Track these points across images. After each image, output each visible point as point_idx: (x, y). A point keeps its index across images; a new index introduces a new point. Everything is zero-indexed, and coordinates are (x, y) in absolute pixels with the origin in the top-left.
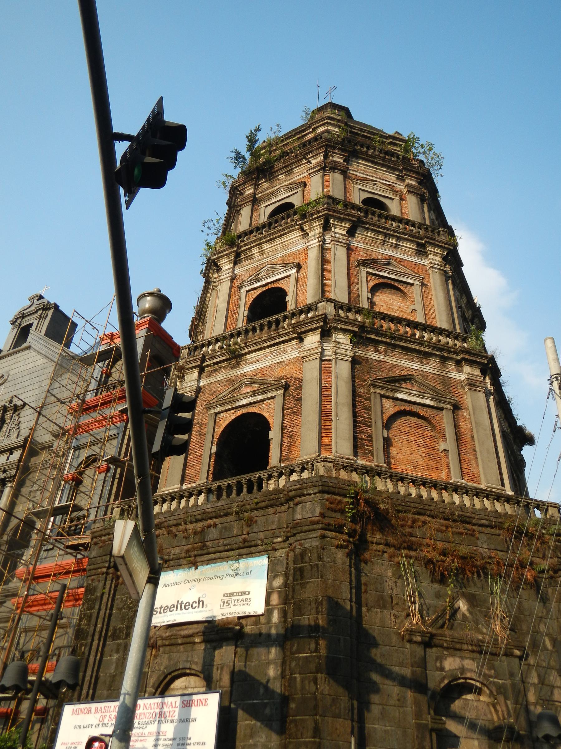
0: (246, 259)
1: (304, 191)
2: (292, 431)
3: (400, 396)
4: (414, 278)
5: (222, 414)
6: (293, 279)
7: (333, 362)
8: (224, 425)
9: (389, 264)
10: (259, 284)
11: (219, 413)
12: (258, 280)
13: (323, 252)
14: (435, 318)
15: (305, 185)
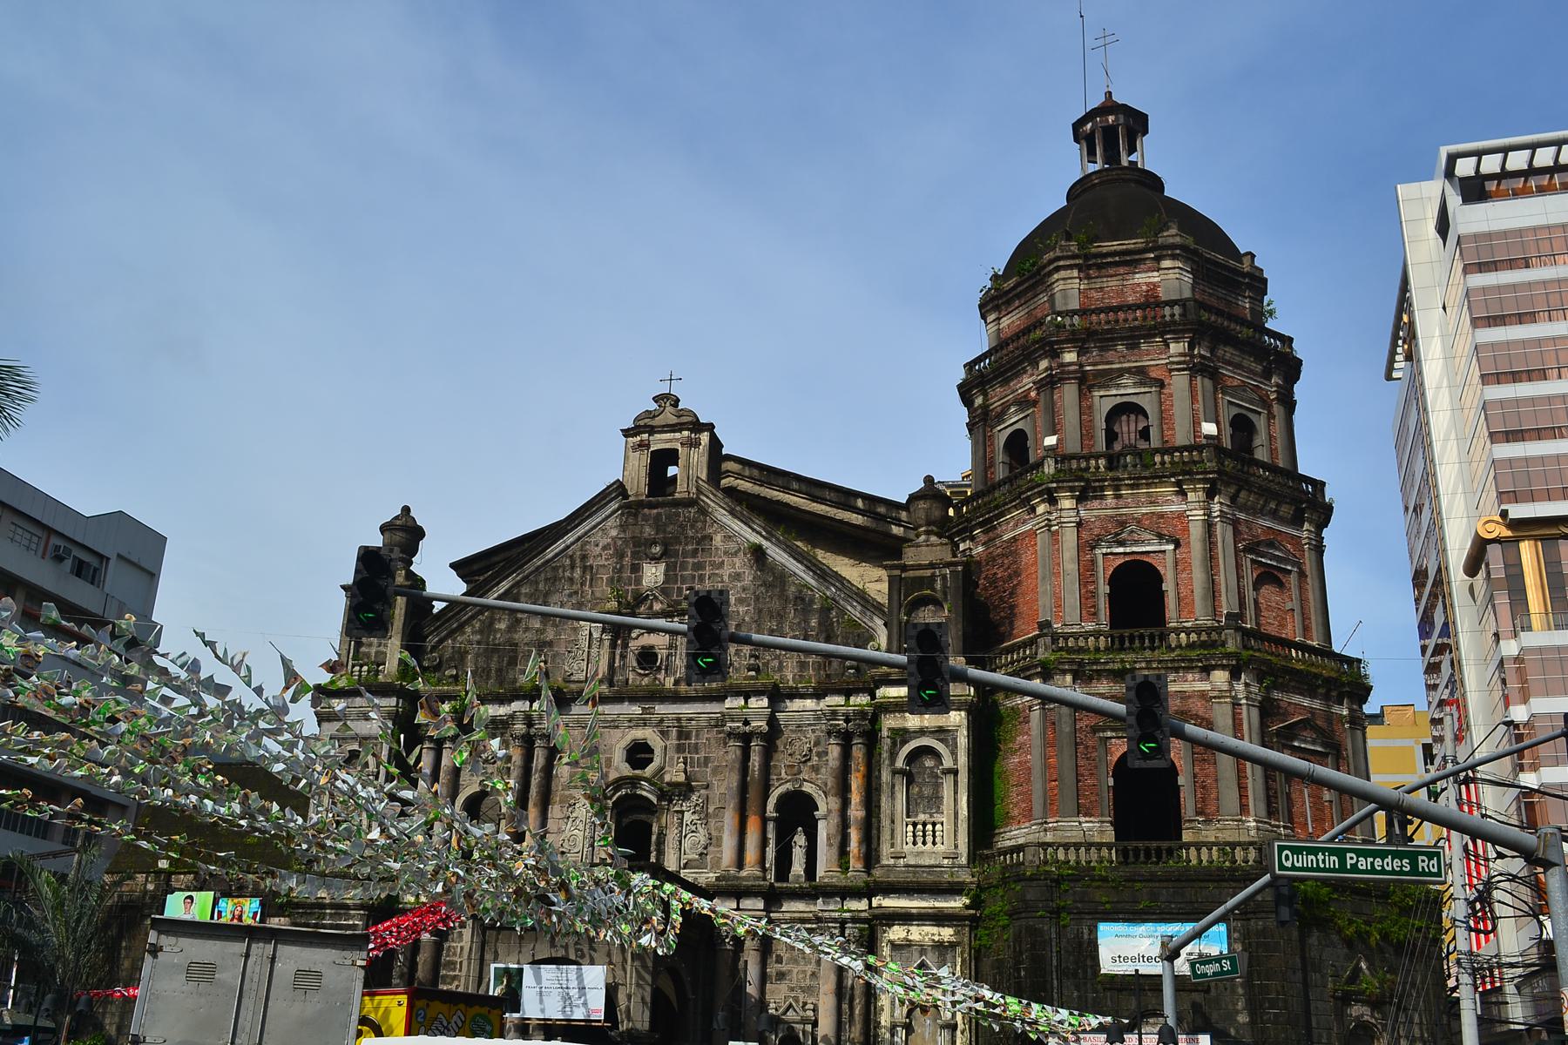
0: (1095, 498)
1: (1160, 393)
2: (1203, 782)
3: (1296, 744)
4: (1294, 564)
5: (1113, 740)
6: (1169, 558)
7: (1244, 707)
8: (1119, 754)
9: (1271, 544)
10: (1121, 550)
11: (1111, 738)
12: (1122, 543)
13: (1209, 526)
14: (1310, 619)
15: (1161, 384)
